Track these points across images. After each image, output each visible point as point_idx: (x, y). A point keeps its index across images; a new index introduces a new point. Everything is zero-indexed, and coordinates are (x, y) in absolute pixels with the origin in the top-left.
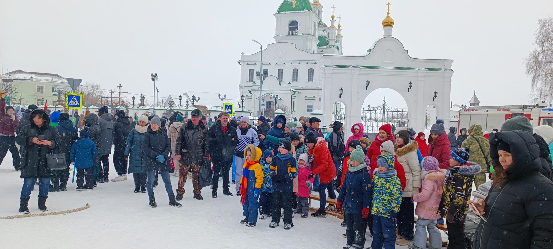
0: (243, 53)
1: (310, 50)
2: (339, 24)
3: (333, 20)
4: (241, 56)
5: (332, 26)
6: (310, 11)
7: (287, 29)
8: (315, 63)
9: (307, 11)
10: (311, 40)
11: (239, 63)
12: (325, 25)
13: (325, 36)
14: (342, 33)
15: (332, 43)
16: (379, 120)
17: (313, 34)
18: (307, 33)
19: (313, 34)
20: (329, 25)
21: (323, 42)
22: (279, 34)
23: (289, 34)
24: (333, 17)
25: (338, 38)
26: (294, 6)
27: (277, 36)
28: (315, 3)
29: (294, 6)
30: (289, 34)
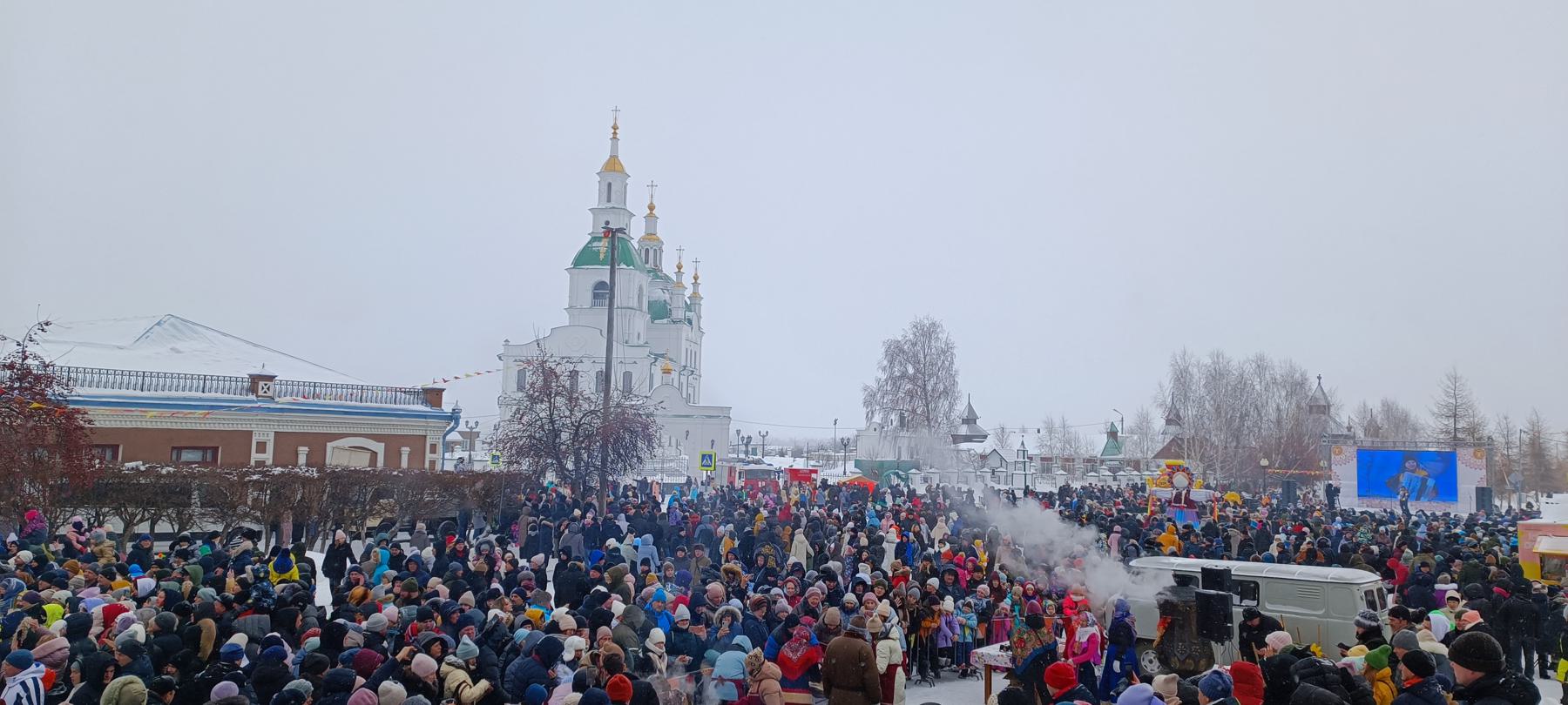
0: (507, 341)
1: (631, 336)
2: (696, 274)
3: (679, 271)
4: (503, 347)
5: (679, 284)
6: (631, 267)
7: (589, 295)
8: (635, 363)
9: (625, 266)
10: (632, 316)
11: (500, 358)
12: (667, 278)
13: (665, 301)
14: (701, 291)
15: (679, 314)
16: (789, 453)
17: (636, 305)
18: (625, 305)
19: (636, 305)
20: (674, 278)
21: (659, 311)
22: (574, 305)
23: (594, 305)
24: (679, 267)
25: (694, 304)
26: (602, 256)
27: (571, 307)
28: (649, 237)
29: (602, 256)
30: (594, 305)
